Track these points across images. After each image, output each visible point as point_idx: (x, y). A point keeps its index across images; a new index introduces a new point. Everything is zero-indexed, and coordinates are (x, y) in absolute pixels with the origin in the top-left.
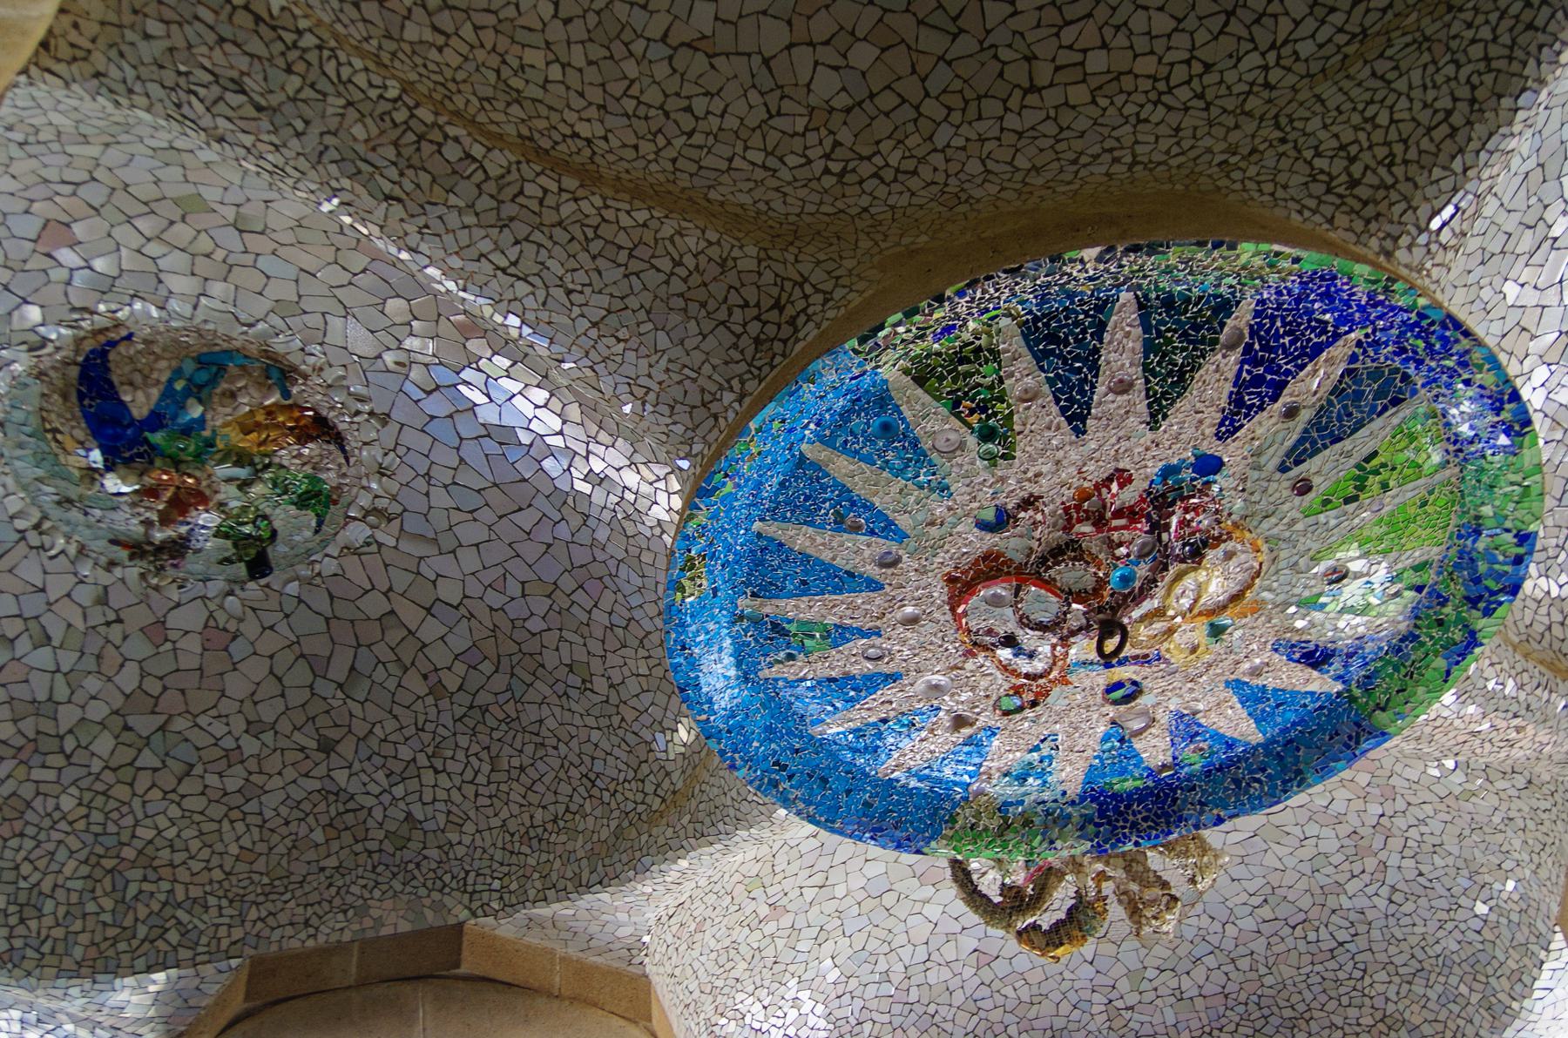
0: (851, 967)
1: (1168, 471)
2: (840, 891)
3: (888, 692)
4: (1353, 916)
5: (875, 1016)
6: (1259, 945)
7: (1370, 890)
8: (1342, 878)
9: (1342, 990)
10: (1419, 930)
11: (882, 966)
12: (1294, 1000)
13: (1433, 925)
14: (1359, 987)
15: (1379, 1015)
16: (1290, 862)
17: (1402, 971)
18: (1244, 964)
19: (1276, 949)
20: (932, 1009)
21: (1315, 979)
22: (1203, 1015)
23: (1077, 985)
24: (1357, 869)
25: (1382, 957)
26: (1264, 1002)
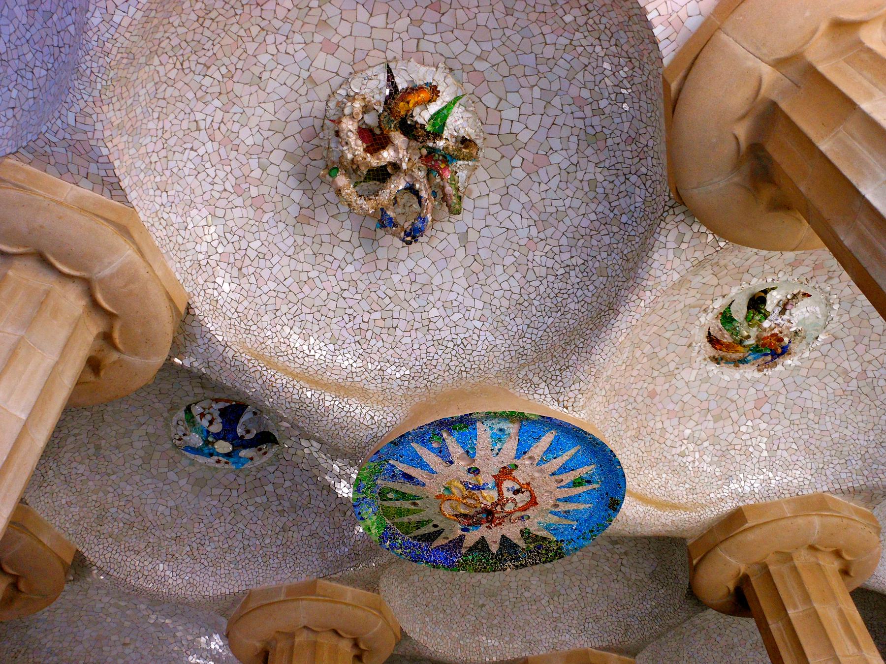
3: (555, 468)
4: (208, 98)
6: (251, 47)
7: (209, 119)
8: (228, 116)
9: (189, 49)
10: (172, 116)
11: (511, 20)
12: (214, 24)
13: (167, 126)
14: (181, 59)
15: (159, 52)
16: (259, 111)
17: (165, 85)
18: (255, 30)
19: (240, 51)
25: (180, 85)
26: (232, 12)
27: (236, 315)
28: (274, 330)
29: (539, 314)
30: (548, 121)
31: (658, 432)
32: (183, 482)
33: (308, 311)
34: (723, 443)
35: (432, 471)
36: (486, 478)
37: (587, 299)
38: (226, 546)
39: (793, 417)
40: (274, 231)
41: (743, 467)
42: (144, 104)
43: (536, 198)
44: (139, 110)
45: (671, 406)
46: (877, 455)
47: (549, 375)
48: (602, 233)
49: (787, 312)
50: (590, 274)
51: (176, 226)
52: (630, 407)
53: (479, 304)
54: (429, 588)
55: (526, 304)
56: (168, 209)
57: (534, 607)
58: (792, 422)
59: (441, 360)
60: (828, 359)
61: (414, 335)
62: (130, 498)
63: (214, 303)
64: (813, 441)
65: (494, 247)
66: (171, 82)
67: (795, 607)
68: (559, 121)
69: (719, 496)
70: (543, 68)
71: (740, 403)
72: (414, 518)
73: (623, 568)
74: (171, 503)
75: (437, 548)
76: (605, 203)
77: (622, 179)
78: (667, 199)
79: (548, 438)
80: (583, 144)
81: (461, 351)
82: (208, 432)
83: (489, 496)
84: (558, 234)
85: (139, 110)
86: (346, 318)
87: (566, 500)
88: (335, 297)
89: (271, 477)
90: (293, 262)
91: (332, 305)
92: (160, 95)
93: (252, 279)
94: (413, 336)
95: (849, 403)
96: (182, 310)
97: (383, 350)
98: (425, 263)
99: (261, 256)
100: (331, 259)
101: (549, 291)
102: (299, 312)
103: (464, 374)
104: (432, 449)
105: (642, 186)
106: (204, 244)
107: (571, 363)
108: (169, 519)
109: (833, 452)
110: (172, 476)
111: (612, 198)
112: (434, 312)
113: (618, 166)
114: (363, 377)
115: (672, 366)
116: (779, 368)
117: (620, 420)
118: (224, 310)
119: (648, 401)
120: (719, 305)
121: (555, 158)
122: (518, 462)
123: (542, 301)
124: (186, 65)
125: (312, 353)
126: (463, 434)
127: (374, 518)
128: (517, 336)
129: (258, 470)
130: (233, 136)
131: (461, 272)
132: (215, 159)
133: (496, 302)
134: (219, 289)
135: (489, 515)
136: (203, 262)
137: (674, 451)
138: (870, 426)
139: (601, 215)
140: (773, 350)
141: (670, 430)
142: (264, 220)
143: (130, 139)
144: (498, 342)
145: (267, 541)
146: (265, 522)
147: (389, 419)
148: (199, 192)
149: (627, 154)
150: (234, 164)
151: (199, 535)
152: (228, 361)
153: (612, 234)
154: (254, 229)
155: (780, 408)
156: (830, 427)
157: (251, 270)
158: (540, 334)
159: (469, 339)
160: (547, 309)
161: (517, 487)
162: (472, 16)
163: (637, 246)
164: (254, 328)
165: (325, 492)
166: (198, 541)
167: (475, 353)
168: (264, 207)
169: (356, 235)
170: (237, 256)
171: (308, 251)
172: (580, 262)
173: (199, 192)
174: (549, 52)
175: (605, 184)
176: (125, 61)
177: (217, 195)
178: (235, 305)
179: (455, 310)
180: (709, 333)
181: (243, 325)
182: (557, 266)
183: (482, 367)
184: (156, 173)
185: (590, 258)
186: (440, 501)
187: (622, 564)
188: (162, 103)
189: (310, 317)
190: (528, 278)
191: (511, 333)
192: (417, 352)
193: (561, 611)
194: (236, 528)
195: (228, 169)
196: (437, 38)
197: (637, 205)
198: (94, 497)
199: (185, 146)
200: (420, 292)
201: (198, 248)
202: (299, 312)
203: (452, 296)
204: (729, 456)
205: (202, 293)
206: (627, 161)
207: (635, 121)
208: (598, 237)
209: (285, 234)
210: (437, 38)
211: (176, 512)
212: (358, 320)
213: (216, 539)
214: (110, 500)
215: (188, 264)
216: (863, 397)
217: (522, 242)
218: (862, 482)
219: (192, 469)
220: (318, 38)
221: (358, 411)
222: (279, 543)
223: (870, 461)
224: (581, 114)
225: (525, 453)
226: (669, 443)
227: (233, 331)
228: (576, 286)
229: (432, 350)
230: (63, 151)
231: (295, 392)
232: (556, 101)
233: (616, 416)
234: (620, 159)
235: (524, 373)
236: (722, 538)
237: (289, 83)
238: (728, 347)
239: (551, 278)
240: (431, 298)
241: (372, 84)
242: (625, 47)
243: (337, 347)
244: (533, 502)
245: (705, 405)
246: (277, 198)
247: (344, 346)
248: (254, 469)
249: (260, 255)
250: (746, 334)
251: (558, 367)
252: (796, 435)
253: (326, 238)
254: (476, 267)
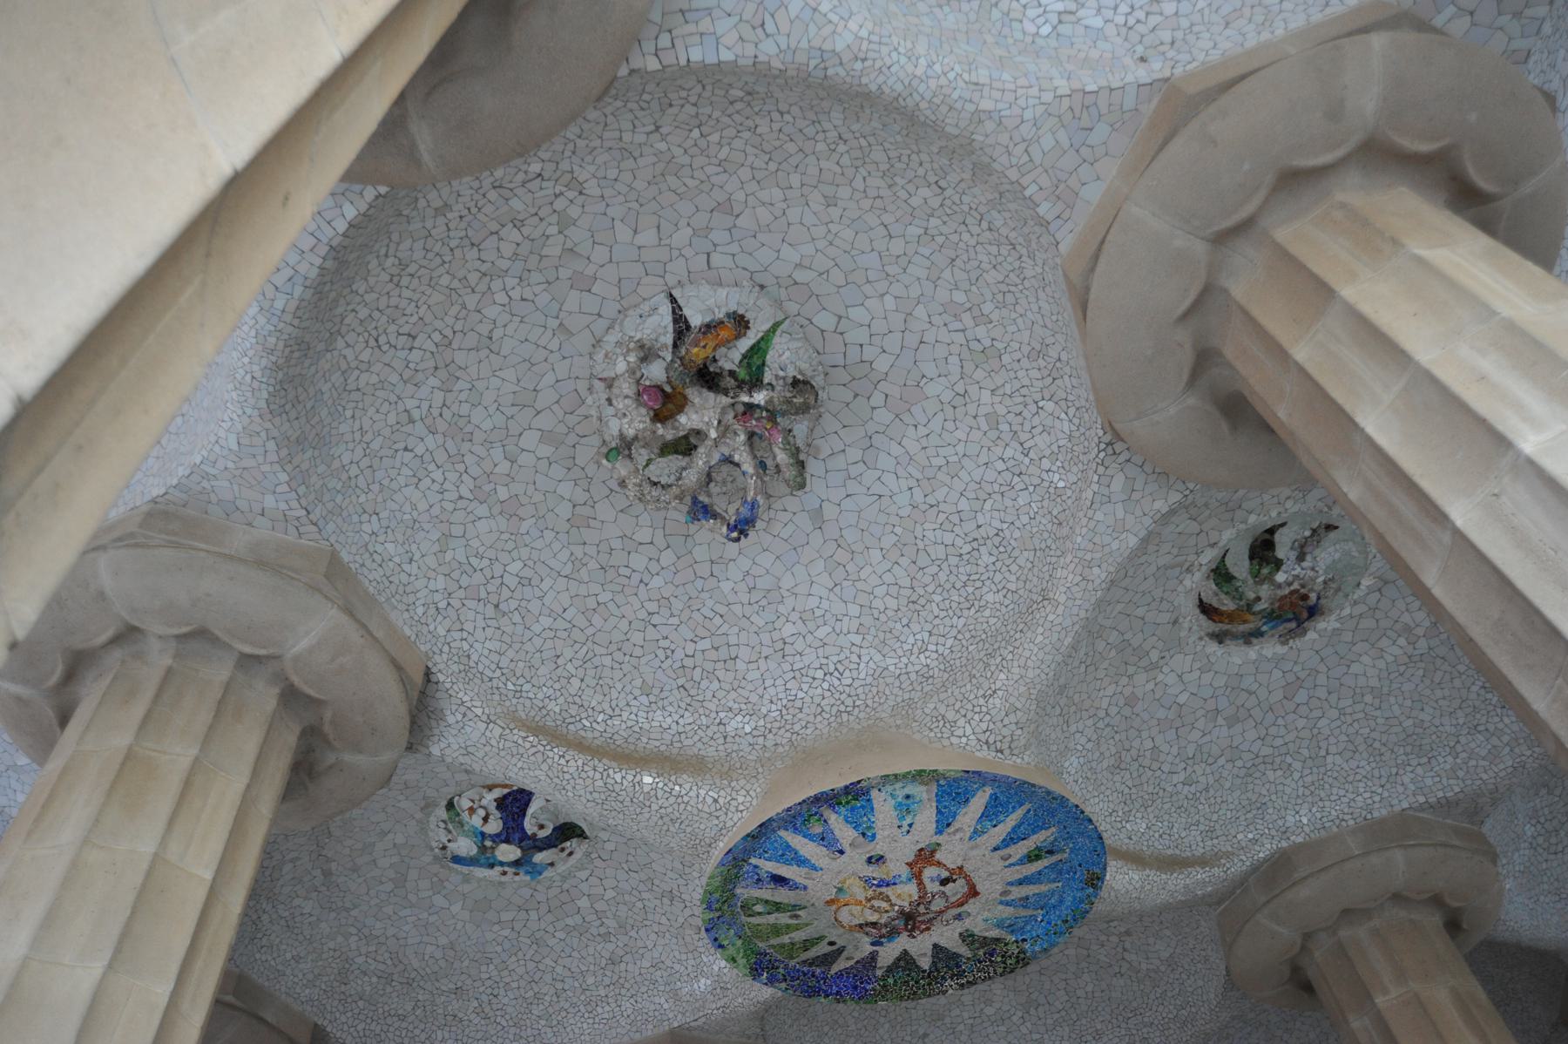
0: (872, 220)
2: (889, 302)
3: (997, 841)
4: (420, 376)
5: (839, 170)
7: (425, 405)
8: (450, 397)
9: (384, 319)
10: (371, 411)
11: (835, 212)
12: (416, 281)
13: (367, 424)
15: (344, 330)
16: (495, 382)
17: (357, 372)
18: (473, 278)
19: (456, 309)
20: (773, 166)
21: (411, 309)
22: (485, 219)
23: (621, 199)
24: (447, 414)
25: (377, 367)
26: (438, 260)
27: (498, 673)
28: (557, 686)
29: (943, 614)
30: (912, 340)
31: (1148, 754)
32: (456, 908)
33: (604, 651)
34: (1246, 756)
35: (815, 868)
36: (897, 866)
37: (1009, 586)
38: (531, 993)
39: (1342, 704)
40: (539, 544)
41: (1280, 788)
42: (330, 402)
43: (912, 446)
44: (324, 413)
45: (1161, 714)
46: (1473, 745)
47: (970, 706)
48: (1017, 488)
49: (1308, 558)
50: (1009, 549)
51: (397, 559)
52: (1101, 724)
53: (854, 610)
54: (841, 1021)
55: (922, 601)
56: (381, 538)
57: (1003, 1028)
58: (1342, 712)
59: (808, 699)
60: (1379, 614)
61: (763, 668)
62: (382, 940)
63: (464, 660)
64: (1374, 735)
65: (863, 525)
66: (364, 367)
67: (1385, 991)
68: (930, 337)
69: (1250, 836)
70: (891, 270)
71: (1263, 693)
72: (799, 936)
73: (1126, 955)
74: (443, 941)
75: (839, 975)
76: (1015, 444)
77: (1033, 408)
78: (1101, 433)
79: (979, 801)
80: (969, 367)
81: (836, 683)
82: (483, 834)
83: (905, 894)
84: (954, 496)
85: (324, 413)
86: (661, 653)
87: (1020, 882)
88: (641, 625)
89: (584, 887)
90: (573, 585)
91: (637, 638)
92: (352, 386)
93: (516, 618)
94: (763, 668)
95: (1421, 672)
96: (418, 678)
97: (721, 694)
98: (766, 560)
99: (525, 582)
100: (627, 572)
101: (952, 578)
102: (591, 654)
103: (845, 716)
104: (811, 838)
105: (1063, 416)
106: (441, 578)
107: (999, 684)
108: (442, 963)
109: (1409, 749)
110: (439, 901)
111: (1023, 437)
112: (788, 630)
113: (1024, 391)
114: (696, 738)
115: (1154, 655)
116: (1311, 635)
117: (1089, 746)
118: (481, 667)
119: (1127, 711)
120: (1209, 557)
121: (931, 389)
122: (940, 839)
123: (945, 595)
124: (382, 339)
125: (617, 711)
126: (853, 810)
127: (739, 943)
128: (916, 650)
129: (564, 878)
130: (461, 423)
131: (820, 564)
132: (441, 457)
133: (877, 603)
134: (470, 639)
135: (911, 921)
136: (442, 605)
137: (1175, 779)
138: (1456, 704)
139: (1012, 462)
140: (1298, 611)
141: (1165, 748)
142: (523, 531)
143: (316, 453)
144: (889, 661)
145: (590, 980)
146: (584, 953)
147: (741, 799)
148: (423, 506)
149: (1035, 374)
150: (469, 459)
151: (488, 983)
152: (493, 742)
153: (1031, 489)
154: (510, 545)
155: (1321, 692)
156: (1397, 711)
157: (513, 604)
158: (950, 642)
159: (846, 662)
160: (954, 605)
161: (945, 874)
162: (778, 213)
163: (1069, 502)
164: (527, 687)
165: (665, 900)
166: (489, 991)
167: (856, 684)
168: (520, 512)
169: (659, 532)
170: (491, 588)
171: (593, 565)
172: (992, 532)
173: (423, 506)
174: (897, 247)
175: (1010, 417)
176: (296, 354)
177: (450, 506)
178: (495, 657)
179: (820, 622)
180: (1201, 600)
181: (510, 686)
182: (959, 542)
183: (869, 702)
184: (358, 492)
185: (1005, 526)
186: (834, 907)
188: (356, 396)
189: (607, 661)
190: (920, 563)
191: (906, 647)
192: (772, 691)
193: (1042, 1029)
194: (541, 967)
195: (461, 467)
196: (735, 248)
197: (1061, 443)
198: (331, 945)
199: (396, 447)
200: (764, 602)
201: (432, 585)
202: (591, 654)
203: (813, 602)
204: (1258, 774)
205: (446, 649)
206: (1036, 383)
208: (1012, 494)
209: (556, 546)
210: (735, 248)
211: (452, 953)
212: (679, 654)
213: (515, 985)
214: (353, 946)
215: (420, 610)
216: (1439, 662)
217: (903, 513)
218: (1457, 789)
219: (466, 888)
220: (564, 273)
221: (692, 794)
222: (607, 981)
223: (1464, 755)
224: (958, 325)
225: (949, 825)
226: (1166, 768)
227: (496, 697)
228: (991, 568)
229: (792, 685)
230: (226, 484)
231: (598, 776)
232: (920, 312)
233: (1083, 740)
234: (1026, 382)
235: (931, 706)
237: (532, 338)
238: (1231, 617)
239: (953, 560)
240: (781, 608)
241: (652, 321)
242: (1004, 231)
243: (652, 698)
244: (973, 892)
245: (1211, 705)
246: (538, 497)
247: (664, 695)
248: (557, 878)
249: (525, 582)
250: (1252, 596)
251: (981, 692)
252: (1351, 730)
253: (616, 544)
254: (841, 555)
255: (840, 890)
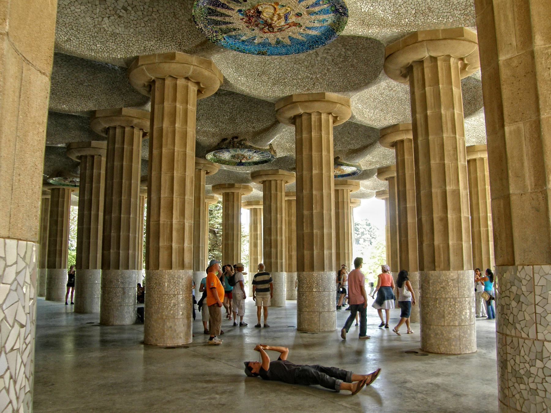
1: (242, 14)
36: (293, 19)
64: (239, 59)
77: (413, 7)
111: (405, 5)
126: (328, 10)
149: (424, 8)
187: (109, 17)
207: (438, 10)
236: (196, 64)
255: (283, 6)
